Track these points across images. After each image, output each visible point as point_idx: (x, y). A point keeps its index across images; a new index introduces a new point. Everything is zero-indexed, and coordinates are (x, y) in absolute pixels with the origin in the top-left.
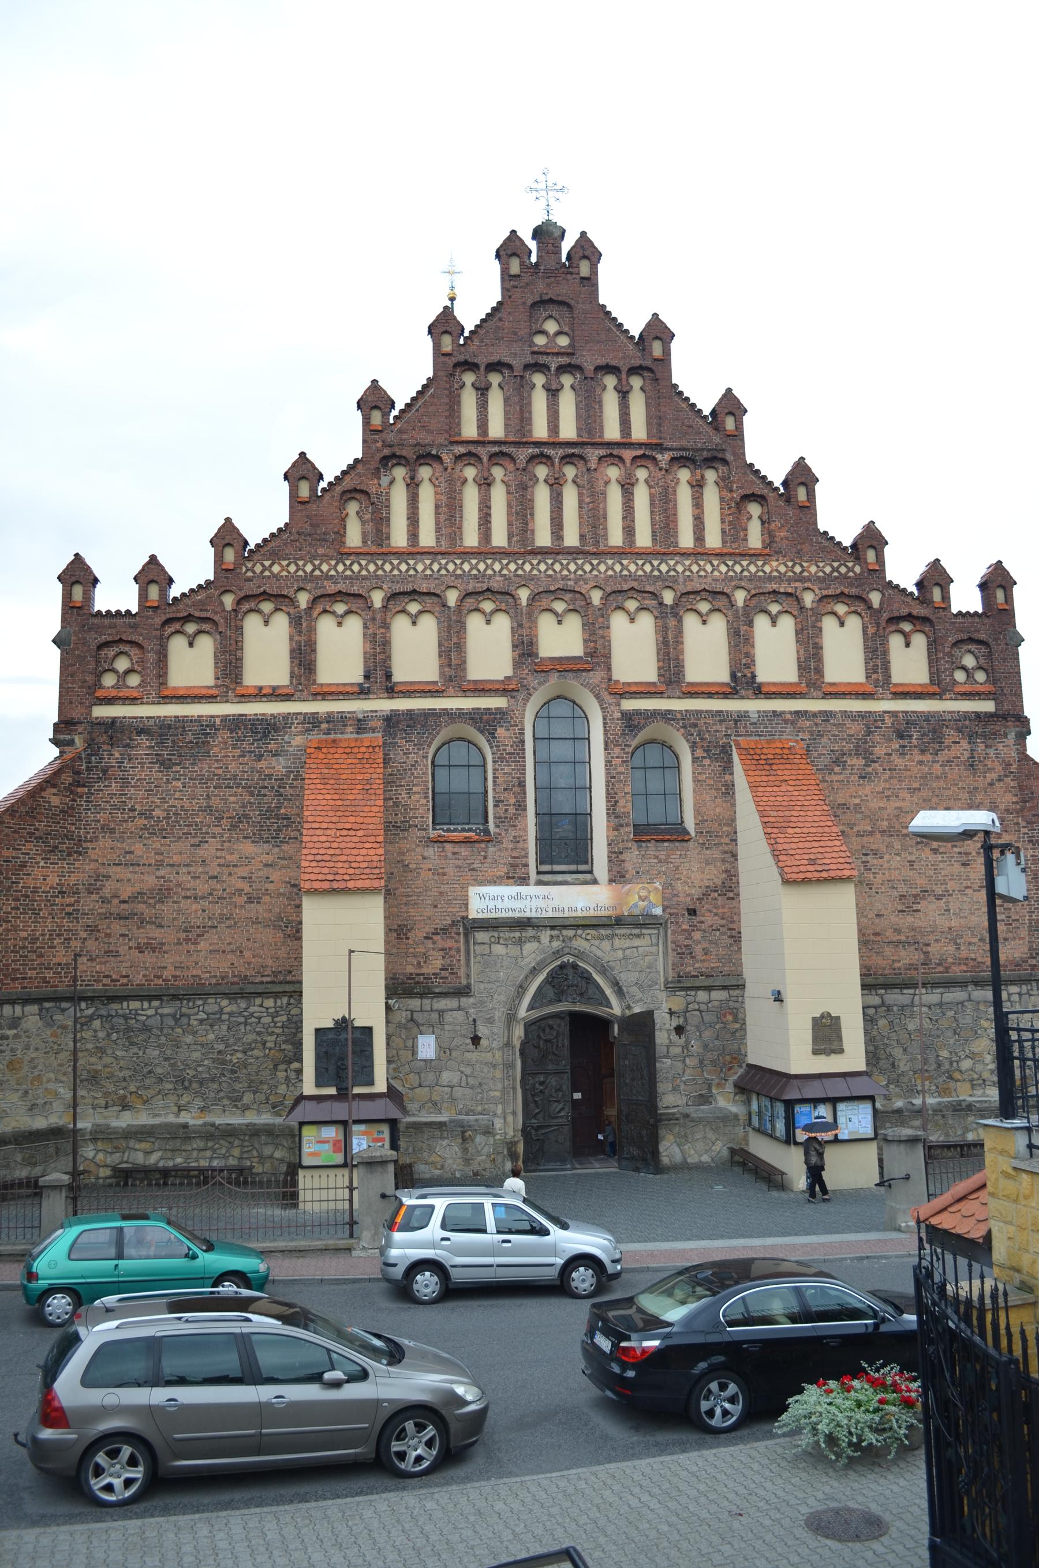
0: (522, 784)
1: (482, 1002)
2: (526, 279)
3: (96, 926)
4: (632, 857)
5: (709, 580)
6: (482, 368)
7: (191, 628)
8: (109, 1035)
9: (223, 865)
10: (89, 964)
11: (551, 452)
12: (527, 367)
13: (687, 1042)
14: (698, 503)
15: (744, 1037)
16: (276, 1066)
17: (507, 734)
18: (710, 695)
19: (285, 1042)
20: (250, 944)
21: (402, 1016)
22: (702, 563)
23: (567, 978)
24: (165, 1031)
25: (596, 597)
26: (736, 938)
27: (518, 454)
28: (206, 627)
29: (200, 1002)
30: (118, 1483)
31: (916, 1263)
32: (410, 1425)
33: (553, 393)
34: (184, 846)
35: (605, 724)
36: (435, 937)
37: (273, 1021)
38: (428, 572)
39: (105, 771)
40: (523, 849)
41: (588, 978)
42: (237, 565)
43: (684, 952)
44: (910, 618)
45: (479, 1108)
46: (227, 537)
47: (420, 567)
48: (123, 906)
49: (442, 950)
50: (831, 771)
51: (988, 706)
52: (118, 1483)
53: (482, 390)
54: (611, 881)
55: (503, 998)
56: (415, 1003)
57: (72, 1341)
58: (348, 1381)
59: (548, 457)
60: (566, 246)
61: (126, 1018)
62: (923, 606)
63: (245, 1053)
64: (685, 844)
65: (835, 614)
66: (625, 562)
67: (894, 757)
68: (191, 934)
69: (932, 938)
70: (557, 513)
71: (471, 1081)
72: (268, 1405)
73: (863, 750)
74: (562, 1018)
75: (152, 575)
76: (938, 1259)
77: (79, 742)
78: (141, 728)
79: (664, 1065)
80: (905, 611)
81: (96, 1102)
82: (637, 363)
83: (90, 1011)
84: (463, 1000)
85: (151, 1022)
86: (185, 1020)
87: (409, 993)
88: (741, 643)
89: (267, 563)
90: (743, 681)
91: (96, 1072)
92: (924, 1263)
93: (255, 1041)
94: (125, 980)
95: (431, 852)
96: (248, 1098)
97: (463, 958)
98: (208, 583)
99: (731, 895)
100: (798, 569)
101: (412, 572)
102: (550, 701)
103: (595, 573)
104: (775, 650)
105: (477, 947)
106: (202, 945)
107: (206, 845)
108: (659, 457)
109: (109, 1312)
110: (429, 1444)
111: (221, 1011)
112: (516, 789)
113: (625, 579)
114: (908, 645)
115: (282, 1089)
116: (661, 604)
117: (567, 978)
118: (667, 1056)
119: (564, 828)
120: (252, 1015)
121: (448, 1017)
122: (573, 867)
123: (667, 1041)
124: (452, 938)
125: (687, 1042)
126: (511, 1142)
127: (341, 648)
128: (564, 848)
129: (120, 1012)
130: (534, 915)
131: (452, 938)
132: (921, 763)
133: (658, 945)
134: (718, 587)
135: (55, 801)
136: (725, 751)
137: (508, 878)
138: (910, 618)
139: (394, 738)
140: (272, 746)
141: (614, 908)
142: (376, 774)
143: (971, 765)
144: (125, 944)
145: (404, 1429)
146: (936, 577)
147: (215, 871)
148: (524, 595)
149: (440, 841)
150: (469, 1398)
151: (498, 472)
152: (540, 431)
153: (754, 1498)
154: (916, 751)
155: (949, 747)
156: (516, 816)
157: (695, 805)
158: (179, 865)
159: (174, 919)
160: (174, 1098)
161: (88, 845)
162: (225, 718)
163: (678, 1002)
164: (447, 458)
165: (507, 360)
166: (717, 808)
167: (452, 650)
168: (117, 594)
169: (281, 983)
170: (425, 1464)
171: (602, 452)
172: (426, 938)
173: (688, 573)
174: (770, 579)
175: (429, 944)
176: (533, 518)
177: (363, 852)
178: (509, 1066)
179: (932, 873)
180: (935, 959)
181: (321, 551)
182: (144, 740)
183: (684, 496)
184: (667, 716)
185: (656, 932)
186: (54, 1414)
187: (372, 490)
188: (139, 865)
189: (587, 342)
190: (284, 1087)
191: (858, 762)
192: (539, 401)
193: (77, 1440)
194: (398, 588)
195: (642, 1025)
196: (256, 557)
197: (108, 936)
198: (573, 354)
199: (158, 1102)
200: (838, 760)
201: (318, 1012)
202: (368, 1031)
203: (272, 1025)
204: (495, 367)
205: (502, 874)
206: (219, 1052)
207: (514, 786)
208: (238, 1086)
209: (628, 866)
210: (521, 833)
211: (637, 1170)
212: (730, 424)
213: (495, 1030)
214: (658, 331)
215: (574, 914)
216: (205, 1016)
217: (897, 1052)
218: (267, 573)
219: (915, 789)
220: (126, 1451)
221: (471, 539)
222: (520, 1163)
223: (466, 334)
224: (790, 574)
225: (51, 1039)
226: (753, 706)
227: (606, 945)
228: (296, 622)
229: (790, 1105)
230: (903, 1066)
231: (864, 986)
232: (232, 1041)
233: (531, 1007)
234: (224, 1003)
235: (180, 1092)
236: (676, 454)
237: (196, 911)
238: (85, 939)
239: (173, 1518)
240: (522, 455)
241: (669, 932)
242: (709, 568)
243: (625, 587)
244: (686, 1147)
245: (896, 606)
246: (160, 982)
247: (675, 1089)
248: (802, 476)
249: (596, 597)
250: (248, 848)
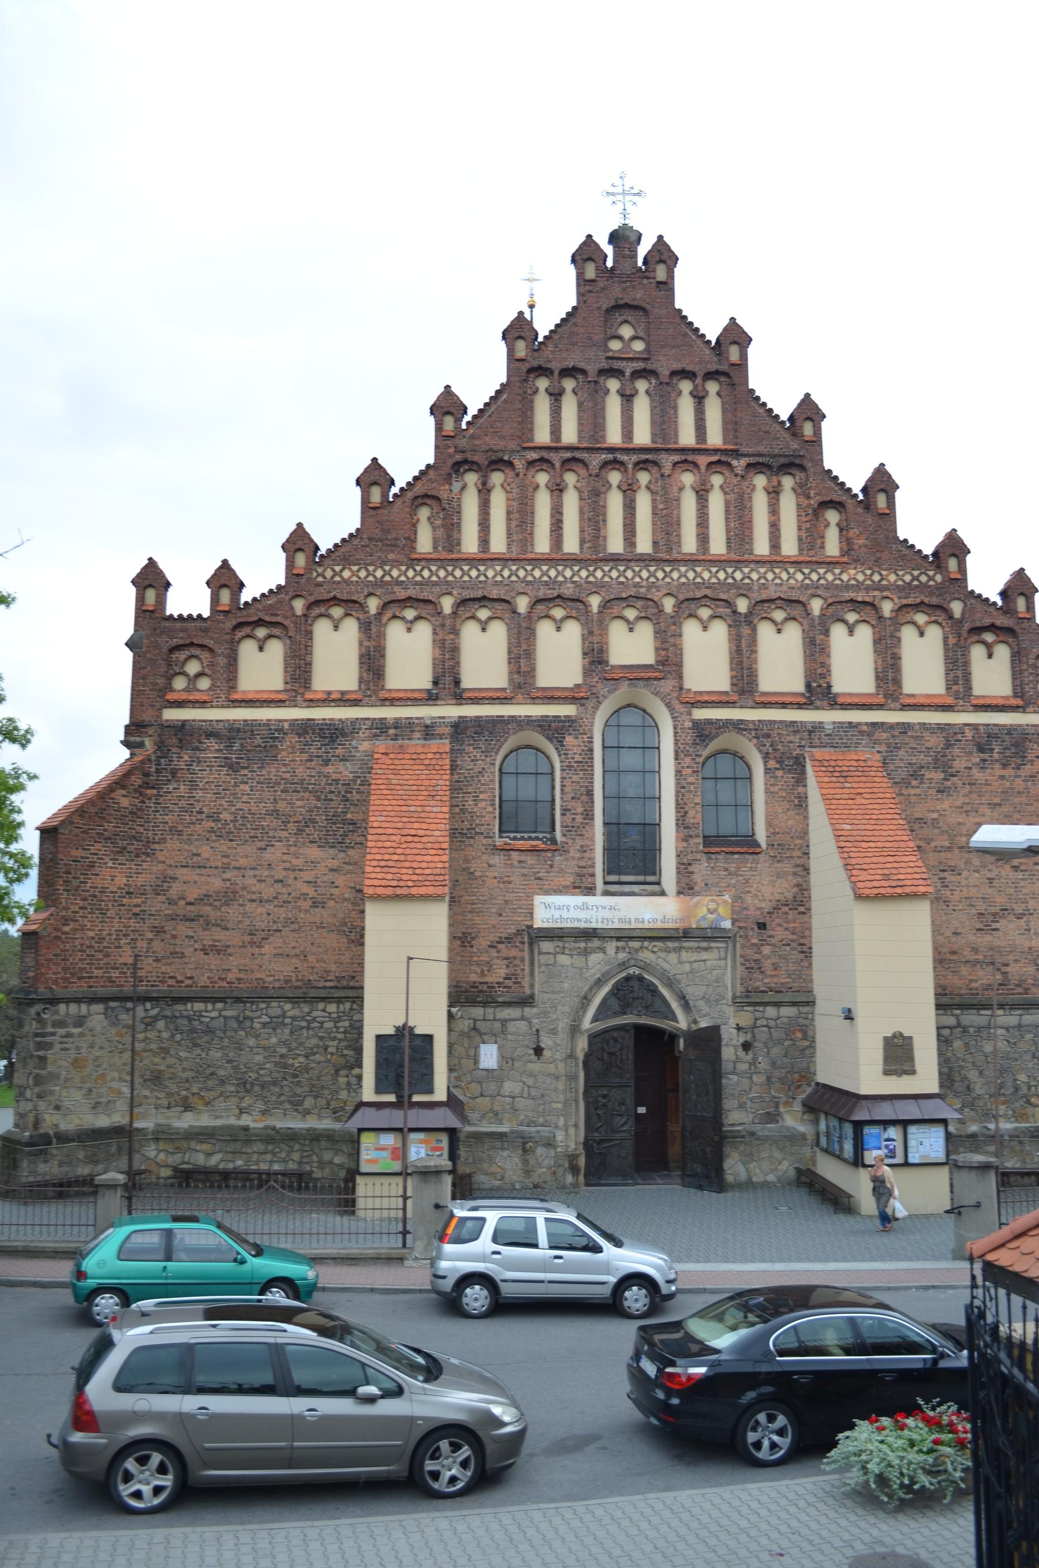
0: (590, 793)
1: (546, 1013)
2: (601, 284)
3: (162, 927)
4: (701, 869)
5: (785, 588)
6: (556, 373)
7: (261, 632)
8: (173, 1036)
9: (289, 869)
10: (155, 964)
11: (624, 458)
12: (602, 372)
13: (755, 1059)
14: (774, 510)
15: (813, 1055)
16: (337, 1071)
17: (576, 742)
18: (784, 705)
19: (347, 1047)
20: (314, 949)
21: (464, 1025)
22: (777, 571)
23: (632, 990)
24: (228, 1033)
25: (669, 605)
26: (807, 953)
27: (592, 461)
28: (276, 631)
29: (263, 1006)
30: (146, 1490)
31: (968, 1301)
32: (444, 1445)
33: (628, 398)
34: (250, 849)
35: (676, 733)
36: (500, 946)
37: (335, 1027)
38: (499, 578)
39: (174, 773)
40: (589, 859)
41: (654, 991)
42: (308, 569)
43: (753, 967)
44: (992, 628)
45: (541, 1120)
46: (299, 542)
47: (490, 573)
48: (189, 908)
49: (506, 959)
50: (908, 784)
52: (146, 1490)
53: (556, 396)
54: (679, 893)
55: (566, 1009)
56: (478, 1012)
57: (104, 1345)
58: (382, 1397)
59: (622, 463)
60: (643, 250)
61: (189, 1019)
63: (307, 1057)
64: (755, 857)
65: (914, 623)
66: (698, 569)
67: (975, 771)
68: (255, 938)
69: (1011, 957)
70: (630, 520)
71: (533, 1092)
72: (300, 1417)
73: (942, 763)
74: (627, 1031)
75: (225, 579)
76: (991, 1299)
77: (148, 743)
78: (210, 731)
79: (730, 1082)
80: (987, 622)
81: (159, 1102)
82: (713, 367)
83: (155, 1012)
84: (527, 1010)
85: (215, 1024)
86: (248, 1023)
87: (473, 1002)
88: (816, 652)
89: (338, 568)
90: (818, 691)
91: (160, 1072)
92: (977, 1303)
93: (317, 1046)
94: (189, 982)
95: (497, 860)
96: (308, 1103)
97: (527, 968)
98: (279, 587)
99: (802, 909)
100: (876, 578)
101: (482, 578)
102: (620, 709)
103: (668, 580)
105: (541, 957)
106: (267, 948)
107: (272, 849)
108: (735, 463)
109: (144, 1316)
110: (464, 1464)
111: (284, 1015)
112: (584, 798)
113: (698, 586)
114: (990, 656)
115: (343, 1095)
116: (735, 612)
117: (632, 990)
118: (733, 1073)
119: (633, 839)
120: (314, 1019)
121: (511, 1027)
122: (640, 878)
123: (733, 1058)
124: (517, 947)
125: (755, 1059)
126: (573, 1155)
127: (410, 654)
128: (632, 859)
129: (185, 1013)
130: (600, 926)
131: (517, 947)
132: (1002, 777)
133: (726, 959)
134: (794, 595)
135: (125, 802)
136: (799, 764)
137: (575, 887)
138: (992, 628)
139: (461, 745)
140: (340, 751)
141: (682, 920)
142: (443, 781)
144: (191, 946)
145: (438, 1449)
147: (280, 874)
148: (595, 602)
149: (506, 850)
150: (506, 1419)
151: (570, 478)
152: (614, 436)
153: (798, 1538)
154: (997, 766)
155: (1032, 761)
156: (584, 825)
157: (766, 817)
158: (245, 869)
159: (239, 922)
160: (236, 1100)
161: (156, 846)
162: (293, 723)
163: (745, 1018)
164: (519, 464)
165: (582, 365)
167: (522, 657)
169: (344, 988)
170: (460, 1485)
171: (676, 458)
172: (490, 946)
173: (763, 581)
174: (847, 587)
175: (493, 953)
176: (605, 525)
177: (428, 858)
178: (572, 1078)
179: (1012, 891)
180: (1014, 979)
181: (391, 556)
182: (213, 744)
183: (760, 502)
184: (739, 726)
185: (724, 945)
186: (84, 1418)
187: (443, 495)
188: (205, 867)
189: (662, 347)
190: (345, 1092)
191: (937, 776)
192: (613, 406)
193: (107, 1445)
194: (468, 594)
195: (708, 1040)
196: (327, 562)
197: (174, 937)
198: (648, 359)
199: (220, 1104)
200: (916, 774)
201: (379, 1019)
202: (429, 1039)
203: (334, 1030)
204: (568, 372)
205: (568, 884)
206: (282, 1056)
207: (581, 795)
208: (299, 1090)
209: (697, 878)
210: (589, 843)
211: (701, 1188)
212: (808, 429)
213: (559, 1042)
214: (735, 336)
215: (641, 926)
216: (268, 1020)
217: (973, 1075)
218: (337, 579)
219: (995, 804)
220: (156, 1458)
221: (542, 545)
222: (581, 1178)
223: (540, 339)
224: (868, 582)
225: (117, 1038)
226: (829, 717)
227: (673, 957)
228: (365, 627)
229: (859, 1126)
230: (979, 1088)
231: (939, 1006)
232: (294, 1045)
233: (595, 1019)
234: (288, 1006)
235: (241, 1095)
236: (752, 460)
237: (261, 914)
238: (151, 940)
239: (199, 1529)
240: (595, 460)
241: (738, 946)
242: (784, 576)
243: (699, 595)
244: (751, 1166)
245: (978, 615)
246: (224, 984)
247: (742, 1106)
248: (882, 482)
249: (669, 605)
250: (314, 852)
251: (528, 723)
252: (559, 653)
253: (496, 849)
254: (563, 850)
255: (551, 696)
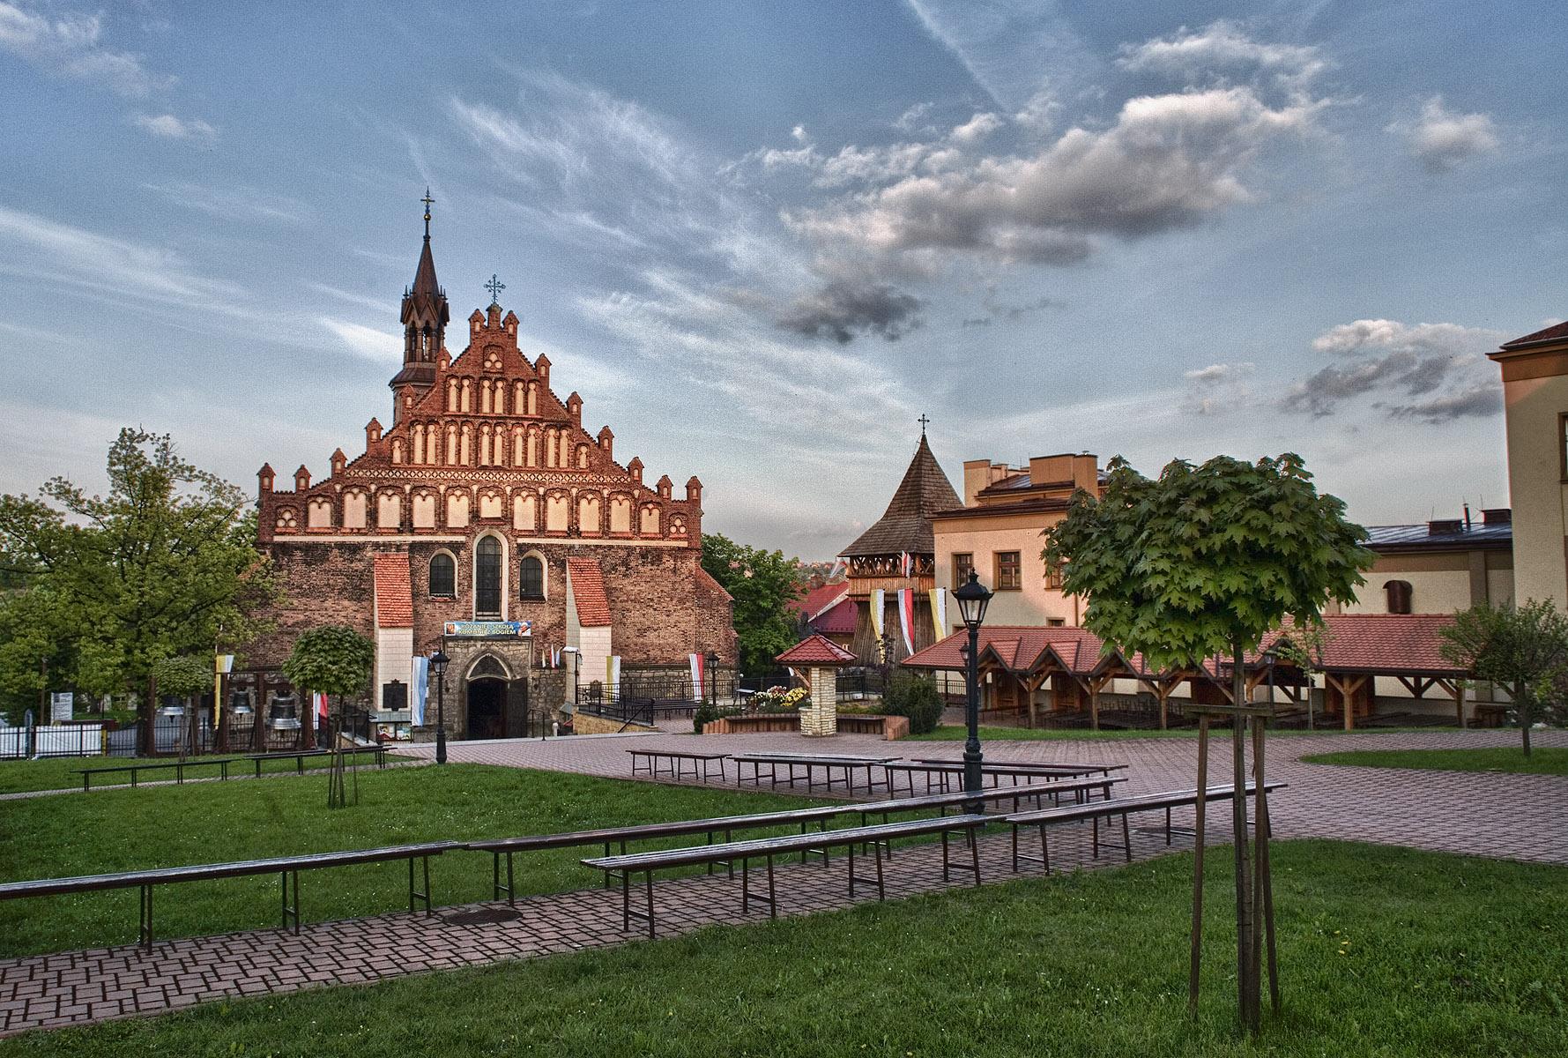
7: (320, 500)
14: (558, 447)
23: (488, 663)
25: (508, 490)
27: (476, 419)
34: (317, 602)
46: (338, 457)
51: (684, 544)
60: (503, 316)
62: (659, 497)
70: (492, 449)
73: (625, 563)
75: (302, 473)
78: (297, 547)
88: (573, 511)
104: (589, 517)
117: (488, 663)
136: (563, 562)
143: (674, 571)
146: (665, 483)
149: (433, 601)
151: (465, 429)
163: (536, 674)
166: (558, 588)
167: (441, 512)
168: (284, 483)
182: (298, 553)
184: (537, 546)
212: (575, 408)
226: (576, 542)
228: (369, 498)
248: (606, 434)
249: (508, 490)
250: (346, 603)
251: (444, 544)
252: (458, 511)
253: (428, 602)
254: (459, 602)
255: (454, 531)
